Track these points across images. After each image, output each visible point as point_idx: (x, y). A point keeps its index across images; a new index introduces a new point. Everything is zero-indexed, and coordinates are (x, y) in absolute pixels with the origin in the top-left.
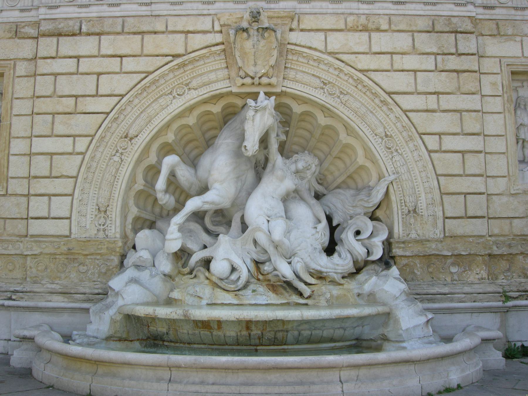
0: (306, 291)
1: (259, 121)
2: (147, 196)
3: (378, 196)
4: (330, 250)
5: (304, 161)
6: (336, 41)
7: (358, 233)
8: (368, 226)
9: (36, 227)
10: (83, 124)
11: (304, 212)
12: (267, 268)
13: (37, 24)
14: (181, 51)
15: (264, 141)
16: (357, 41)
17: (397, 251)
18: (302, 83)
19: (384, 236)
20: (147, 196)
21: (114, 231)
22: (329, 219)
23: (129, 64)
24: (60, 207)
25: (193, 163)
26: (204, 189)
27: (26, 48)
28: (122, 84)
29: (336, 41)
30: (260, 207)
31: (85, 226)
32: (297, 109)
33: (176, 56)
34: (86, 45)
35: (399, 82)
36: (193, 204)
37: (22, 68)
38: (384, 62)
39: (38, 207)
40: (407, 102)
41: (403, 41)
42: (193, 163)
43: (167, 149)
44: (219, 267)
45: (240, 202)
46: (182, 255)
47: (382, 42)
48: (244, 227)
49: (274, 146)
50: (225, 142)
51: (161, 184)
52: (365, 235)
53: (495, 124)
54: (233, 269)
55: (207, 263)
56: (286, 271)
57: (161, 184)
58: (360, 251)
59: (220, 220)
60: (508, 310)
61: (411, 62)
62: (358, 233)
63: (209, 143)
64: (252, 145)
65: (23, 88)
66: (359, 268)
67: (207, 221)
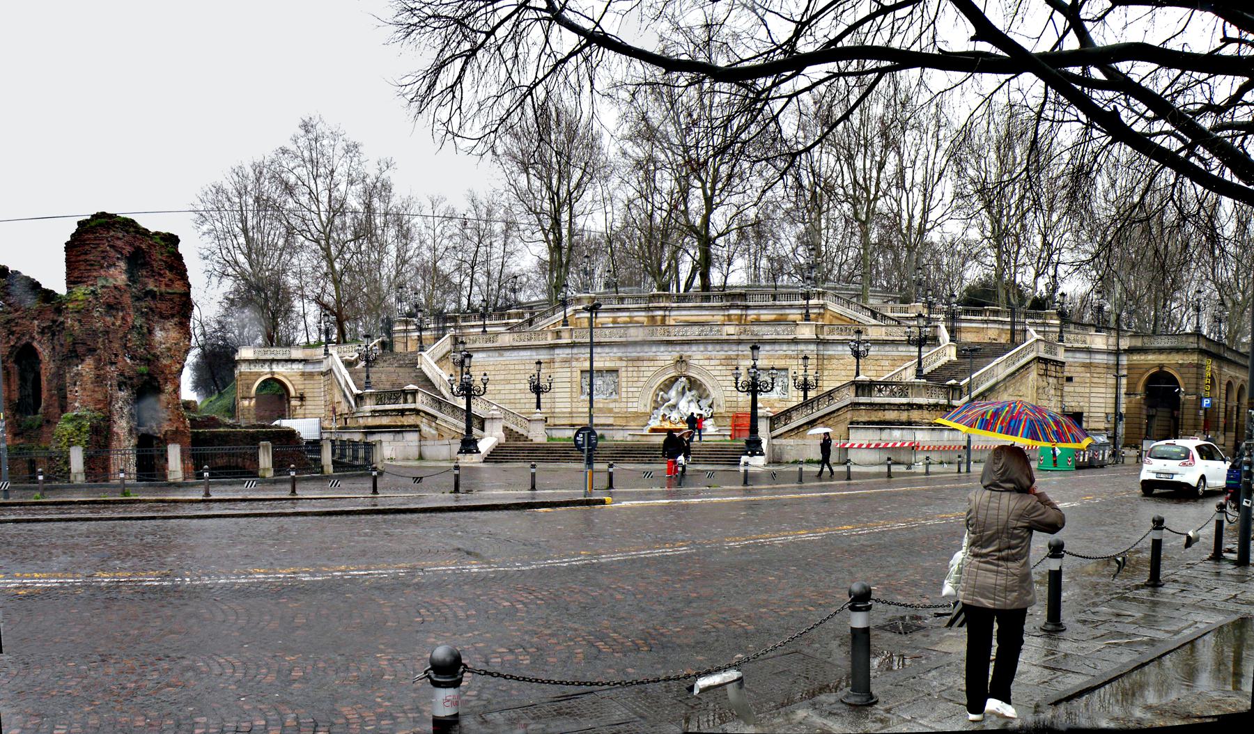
2: (656, 401)
5: (694, 392)
6: (701, 362)
10: (640, 384)
16: (706, 362)
18: (692, 374)
20: (656, 401)
24: (635, 405)
27: (624, 364)
28: (649, 374)
29: (701, 362)
31: (642, 409)
34: (640, 363)
39: (630, 405)
41: (718, 362)
43: (661, 390)
46: (664, 415)
47: (713, 362)
59: (674, 407)
65: (624, 374)
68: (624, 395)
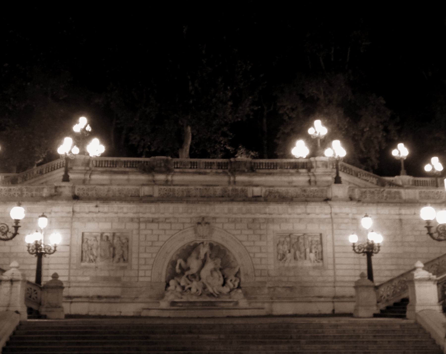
0: (216, 296)
1: (204, 250)
3: (237, 270)
4: (224, 284)
7: (231, 280)
8: (234, 279)
9: (141, 279)
11: (217, 275)
12: (206, 290)
13: (139, 218)
14: (182, 228)
15: (206, 255)
16: (232, 226)
17: (241, 286)
18: (217, 238)
19: (238, 281)
21: (163, 280)
22: (223, 276)
23: (167, 232)
25: (185, 261)
26: (189, 269)
27: (135, 226)
29: (226, 226)
30: (205, 273)
32: (215, 245)
33: (181, 230)
34: (154, 226)
35: (243, 238)
36: (187, 273)
37: (135, 232)
38: (239, 232)
39: (141, 273)
40: (245, 244)
42: (185, 261)
44: (194, 290)
45: (199, 272)
47: (238, 226)
48: (200, 279)
49: (208, 255)
50: (194, 254)
51: (177, 267)
52: (233, 281)
53: (271, 249)
54: (197, 290)
55: (190, 289)
56: (211, 290)
57: (177, 267)
58: (232, 286)
60: (273, 302)
61: (247, 232)
62: (231, 280)
63: (189, 254)
64: (202, 256)
66: (231, 290)
67: (189, 277)
68: (134, 262)
